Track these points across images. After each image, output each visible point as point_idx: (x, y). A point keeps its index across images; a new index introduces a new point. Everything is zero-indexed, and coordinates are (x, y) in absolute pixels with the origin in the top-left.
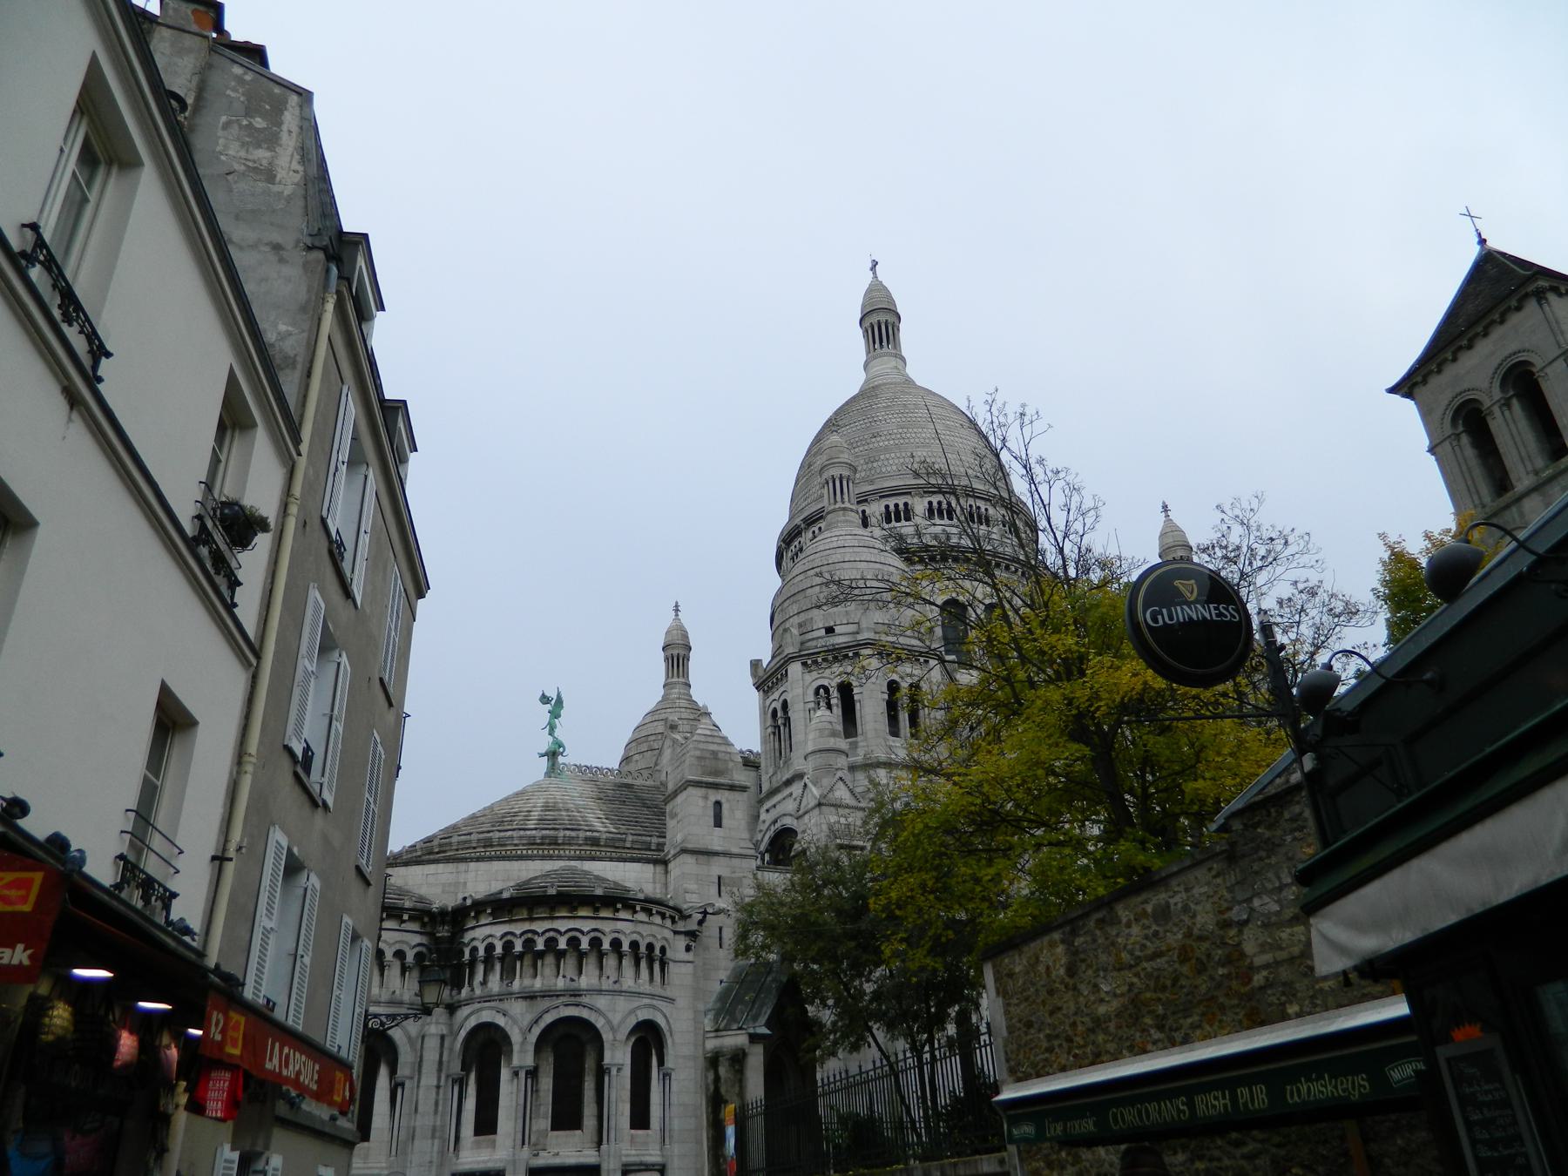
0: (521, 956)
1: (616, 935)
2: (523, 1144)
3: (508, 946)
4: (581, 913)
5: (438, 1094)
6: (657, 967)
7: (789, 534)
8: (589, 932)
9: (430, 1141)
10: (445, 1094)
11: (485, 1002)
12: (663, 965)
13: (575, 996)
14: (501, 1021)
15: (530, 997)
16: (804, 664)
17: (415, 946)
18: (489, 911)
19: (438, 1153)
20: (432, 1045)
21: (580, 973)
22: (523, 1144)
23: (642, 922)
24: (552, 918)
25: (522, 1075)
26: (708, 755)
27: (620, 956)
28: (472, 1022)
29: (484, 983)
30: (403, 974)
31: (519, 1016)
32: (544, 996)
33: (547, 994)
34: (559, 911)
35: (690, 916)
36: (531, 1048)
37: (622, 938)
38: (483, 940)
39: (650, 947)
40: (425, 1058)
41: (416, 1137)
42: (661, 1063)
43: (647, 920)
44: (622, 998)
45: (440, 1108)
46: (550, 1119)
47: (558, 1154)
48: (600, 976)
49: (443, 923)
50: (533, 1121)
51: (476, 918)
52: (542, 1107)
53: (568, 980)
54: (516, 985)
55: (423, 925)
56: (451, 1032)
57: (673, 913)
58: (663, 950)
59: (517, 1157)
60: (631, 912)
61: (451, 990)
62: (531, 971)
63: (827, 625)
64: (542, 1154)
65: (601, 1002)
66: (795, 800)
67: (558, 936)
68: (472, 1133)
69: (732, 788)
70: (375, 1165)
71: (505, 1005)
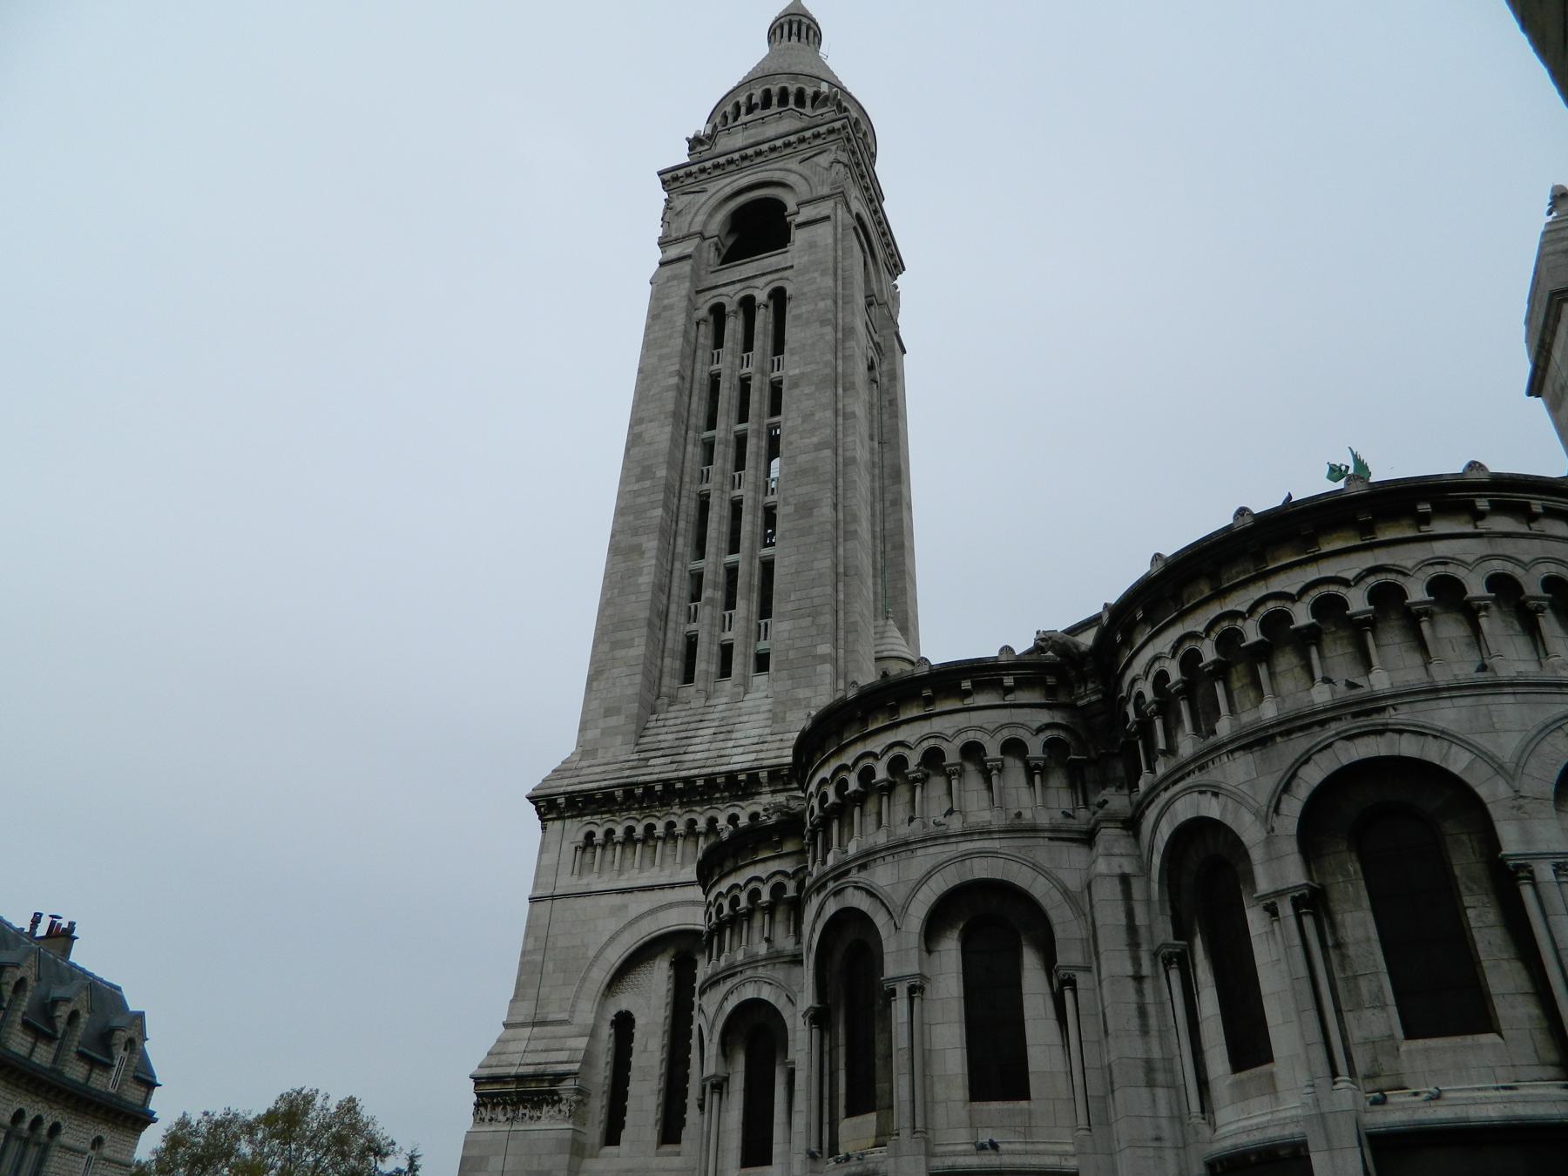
0: (1221, 670)
1: (1440, 569)
2: (1334, 1073)
3: (1190, 661)
4: (1326, 548)
5: (1140, 992)
8: (1359, 579)
9: (1145, 1093)
10: (1157, 990)
11: (1175, 783)
13: (1368, 713)
14: (1212, 809)
15: (1258, 740)
17: (1040, 730)
18: (1140, 615)
19: (1172, 1118)
20: (1107, 893)
21: (1368, 666)
22: (1334, 1073)
24: (1265, 576)
25: (1286, 909)
27: (1470, 613)
28: (1165, 832)
29: (1171, 750)
30: (1031, 782)
31: (1244, 788)
32: (1288, 733)
33: (1291, 726)
34: (1274, 560)
36: (1290, 847)
37: (1460, 573)
38: (1147, 673)
40: (1098, 924)
41: (1116, 1086)
43: (1524, 529)
44: (1511, 699)
45: (1153, 1022)
46: (1393, 1010)
47: (1437, 1096)
48: (1427, 662)
49: (1083, 680)
50: (1349, 1018)
51: (1128, 641)
52: (1363, 984)
53: (1341, 687)
54: (1224, 727)
55: (1050, 691)
56: (1141, 868)
59: (1325, 1109)
60: (1466, 518)
61: (1129, 795)
62: (1252, 695)
64: (1394, 1098)
65: (1446, 715)
67: (1288, 606)
68: (1227, 1066)
70: (1049, 1147)
71: (1213, 775)
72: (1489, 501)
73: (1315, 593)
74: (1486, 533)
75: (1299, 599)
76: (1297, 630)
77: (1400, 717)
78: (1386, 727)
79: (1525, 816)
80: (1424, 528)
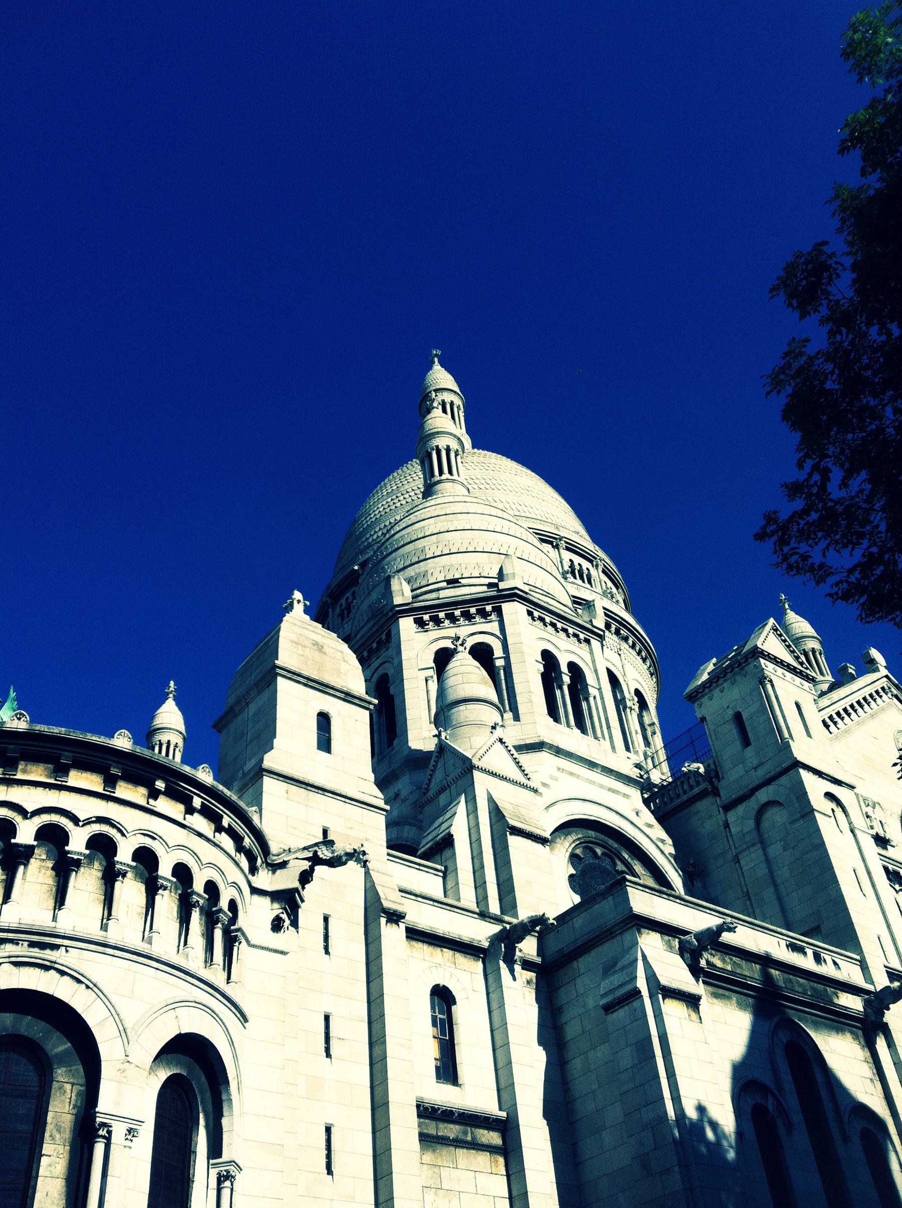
1: (148, 842)
6: (218, 934)
7: (340, 584)
8: (88, 822)
12: (230, 941)
13: (43, 946)
16: (420, 623)
23: (200, 835)
26: (308, 643)
27: (152, 888)
34: (24, 771)
35: (283, 865)
39: (211, 888)
42: (215, 1150)
43: (211, 836)
57: (256, 850)
58: (233, 905)
63: (450, 577)
66: (404, 801)
67: (17, 818)
69: (348, 697)
72: (202, 802)
73: (46, 818)
74: (189, 827)
75: (31, 817)
76: (17, 845)
77: (66, 959)
78: (53, 965)
79: (124, 1080)
80: (151, 801)
